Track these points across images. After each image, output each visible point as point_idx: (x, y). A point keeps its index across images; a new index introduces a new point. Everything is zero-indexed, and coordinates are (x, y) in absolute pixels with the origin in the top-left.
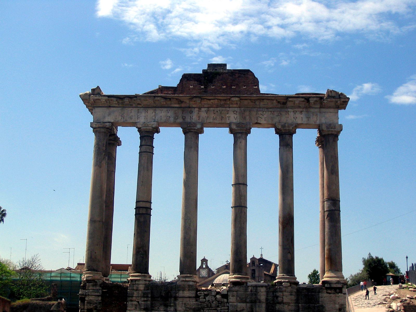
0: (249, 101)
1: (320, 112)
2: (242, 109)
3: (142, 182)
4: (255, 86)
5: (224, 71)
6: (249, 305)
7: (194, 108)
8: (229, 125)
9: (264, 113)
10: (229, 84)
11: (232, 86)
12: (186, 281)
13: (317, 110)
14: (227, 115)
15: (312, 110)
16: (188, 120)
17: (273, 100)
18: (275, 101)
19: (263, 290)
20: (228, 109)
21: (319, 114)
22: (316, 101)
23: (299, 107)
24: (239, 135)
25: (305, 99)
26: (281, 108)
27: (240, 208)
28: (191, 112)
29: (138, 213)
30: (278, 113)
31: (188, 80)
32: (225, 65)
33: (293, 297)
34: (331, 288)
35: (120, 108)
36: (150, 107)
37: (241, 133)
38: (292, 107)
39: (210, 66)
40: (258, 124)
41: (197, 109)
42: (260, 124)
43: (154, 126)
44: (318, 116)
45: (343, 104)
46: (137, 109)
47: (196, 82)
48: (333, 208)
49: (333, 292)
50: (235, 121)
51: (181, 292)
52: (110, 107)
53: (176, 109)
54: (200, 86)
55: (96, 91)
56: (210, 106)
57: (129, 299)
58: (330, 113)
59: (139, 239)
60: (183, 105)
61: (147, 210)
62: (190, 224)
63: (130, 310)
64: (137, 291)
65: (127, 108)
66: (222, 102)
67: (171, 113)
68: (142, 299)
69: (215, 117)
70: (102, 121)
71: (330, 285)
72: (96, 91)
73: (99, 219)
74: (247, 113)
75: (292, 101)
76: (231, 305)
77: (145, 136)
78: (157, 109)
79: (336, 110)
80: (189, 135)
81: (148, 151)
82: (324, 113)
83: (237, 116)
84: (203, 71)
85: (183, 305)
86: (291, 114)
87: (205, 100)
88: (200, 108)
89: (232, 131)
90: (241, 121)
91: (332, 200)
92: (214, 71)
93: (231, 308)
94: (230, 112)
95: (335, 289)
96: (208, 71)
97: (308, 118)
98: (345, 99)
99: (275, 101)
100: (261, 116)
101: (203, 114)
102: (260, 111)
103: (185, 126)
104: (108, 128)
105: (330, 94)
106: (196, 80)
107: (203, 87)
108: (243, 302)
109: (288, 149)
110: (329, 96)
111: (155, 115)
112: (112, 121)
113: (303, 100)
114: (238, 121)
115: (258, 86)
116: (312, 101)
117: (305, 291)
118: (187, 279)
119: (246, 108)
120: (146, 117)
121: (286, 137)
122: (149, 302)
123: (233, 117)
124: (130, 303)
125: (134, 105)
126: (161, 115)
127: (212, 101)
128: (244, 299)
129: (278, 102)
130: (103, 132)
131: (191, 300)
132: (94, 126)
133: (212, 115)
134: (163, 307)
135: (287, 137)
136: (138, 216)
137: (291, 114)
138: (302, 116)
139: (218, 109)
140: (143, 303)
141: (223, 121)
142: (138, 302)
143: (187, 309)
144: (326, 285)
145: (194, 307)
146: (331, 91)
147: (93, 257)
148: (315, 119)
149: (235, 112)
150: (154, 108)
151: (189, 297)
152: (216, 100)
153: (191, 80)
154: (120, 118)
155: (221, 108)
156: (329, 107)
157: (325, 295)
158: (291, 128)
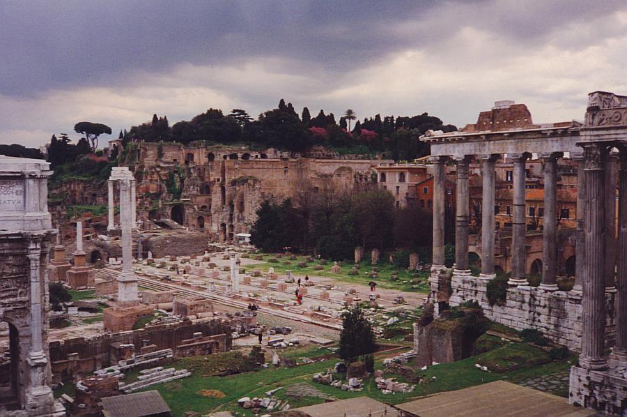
6: (519, 303)
15: (565, 138)
28: (485, 145)
41: (488, 142)
74: (520, 144)
78: (465, 144)
83: (513, 147)
86: (550, 143)
88: (489, 141)
92: (498, 108)
95: (576, 300)
97: (562, 146)
101: (492, 147)
104: (439, 161)
133: (497, 147)
137: (550, 143)
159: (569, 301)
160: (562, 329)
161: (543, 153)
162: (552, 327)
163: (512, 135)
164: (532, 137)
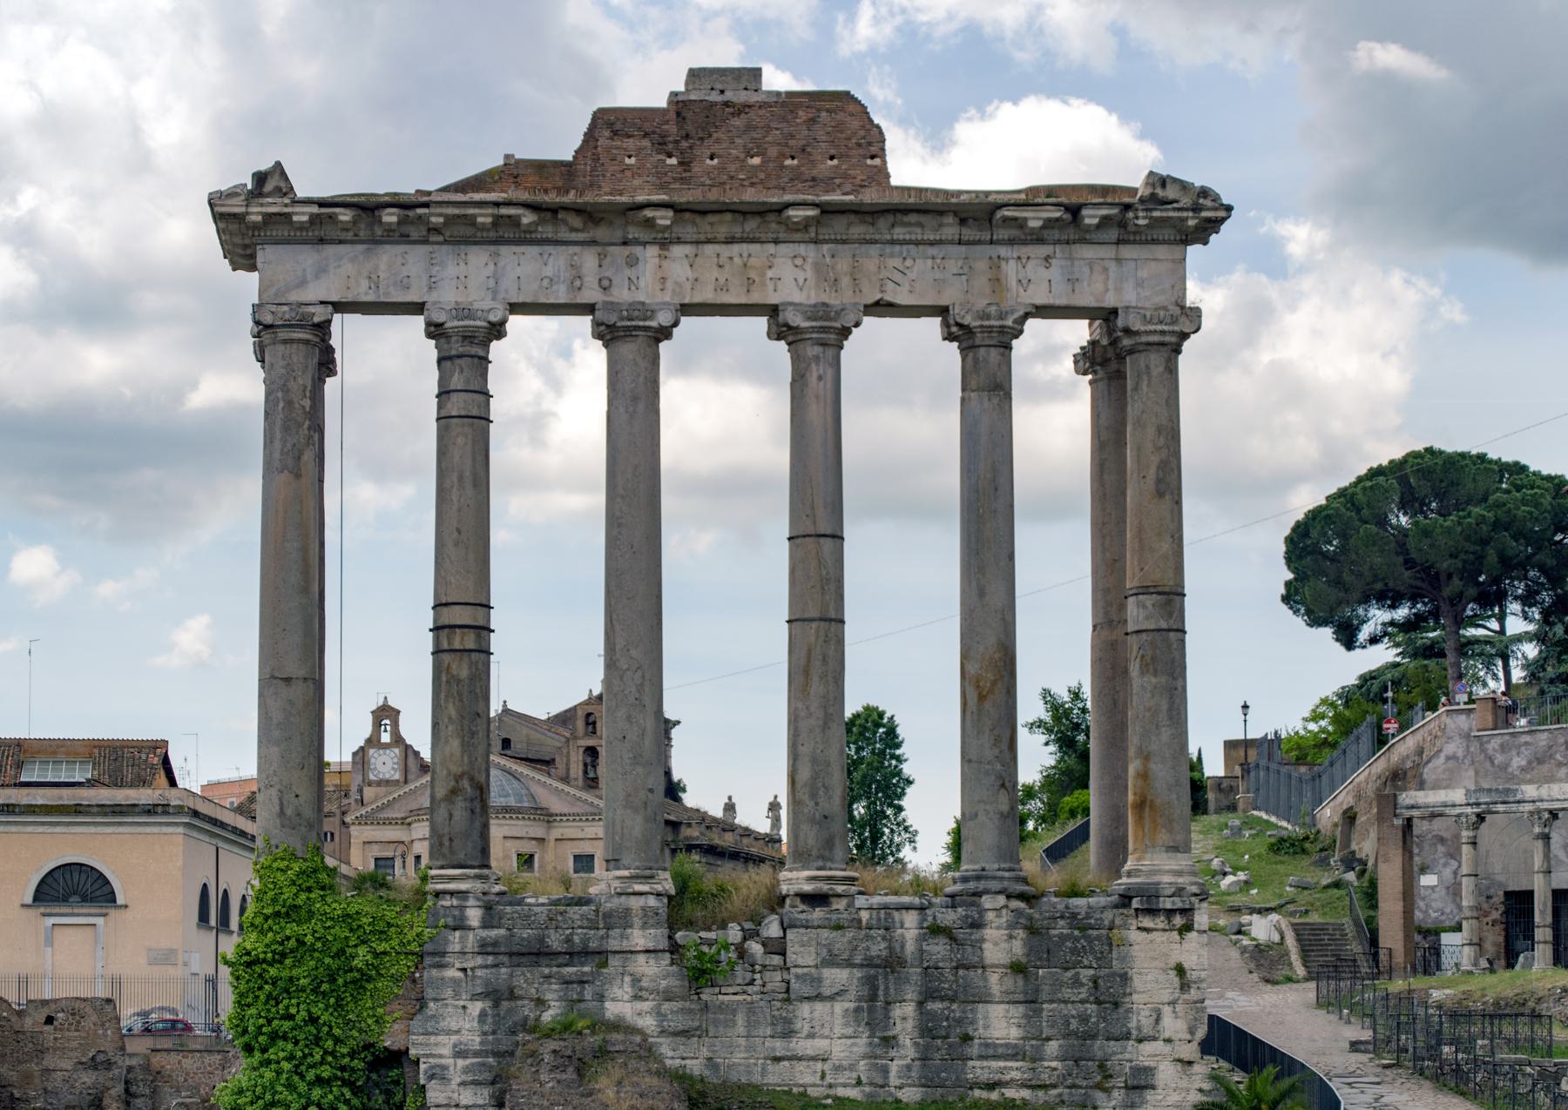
0: (852, 217)
1: (1118, 260)
2: (826, 247)
3: (459, 531)
4: (872, 157)
5: (754, 98)
6: (858, 973)
7: (644, 244)
8: (772, 311)
9: (909, 263)
10: (773, 152)
11: (783, 156)
12: (635, 894)
13: (1108, 252)
14: (770, 274)
15: (1088, 252)
16: (622, 294)
17: (941, 213)
18: (950, 219)
19: (911, 919)
20: (771, 248)
21: (1112, 266)
22: (1105, 218)
23: (1040, 241)
24: (812, 351)
25: (1067, 208)
26: (969, 243)
27: (822, 624)
28: (632, 262)
29: (445, 646)
30: (960, 263)
31: (615, 133)
32: (756, 73)
33: (1018, 948)
34: (1152, 912)
35: (360, 247)
36: (475, 243)
37: (824, 345)
38: (1011, 242)
39: (695, 75)
40: (882, 308)
41: (652, 251)
42: (890, 305)
43: (493, 318)
44: (1112, 274)
45: (1205, 229)
46: (422, 250)
47: (646, 143)
48: (1164, 625)
49: (1161, 926)
50: (798, 297)
51: (616, 932)
52: (322, 241)
53: (577, 249)
54: (662, 157)
55: (270, 181)
56: (702, 237)
57: (428, 960)
58: (1153, 264)
59: (455, 744)
60: (601, 233)
61: (478, 636)
62: (642, 685)
63: (435, 1000)
64: (457, 934)
65: (388, 247)
66: (751, 225)
67: (557, 261)
68: (479, 960)
69: (722, 281)
70: (294, 297)
71: (1148, 902)
72: (270, 181)
73: (302, 673)
75: (1016, 219)
76: (797, 976)
77: (460, 356)
78: (504, 250)
79: (1178, 248)
80: (628, 349)
81: (475, 412)
82: (1132, 264)
83: (809, 274)
84: (674, 94)
85: (627, 979)
86: (1011, 270)
87: (687, 215)
88: (664, 244)
89: (781, 331)
90: (824, 298)
91: (1159, 593)
92: (715, 97)
93: (794, 985)
94: (778, 261)
95: (1170, 913)
96: (693, 97)
97: (1072, 281)
98: (1216, 209)
99: (950, 219)
100: (897, 277)
102: (892, 256)
103: (612, 319)
105: (1159, 191)
106: (646, 135)
107: (674, 161)
108: (838, 965)
109: (995, 401)
110: (1153, 201)
111: (495, 272)
112: (335, 299)
113: (1058, 215)
114: (809, 296)
115: (884, 162)
116: (1090, 217)
117: (1061, 923)
118: (638, 888)
119: (840, 247)
120: (462, 282)
121: (984, 348)
122: (503, 970)
123: (791, 276)
124: (434, 972)
125: (415, 234)
126: (519, 271)
127: (711, 218)
128: (845, 956)
129: (963, 222)
130: (300, 341)
131: (652, 962)
132: (268, 319)
134: (555, 987)
135: (994, 353)
136: (446, 658)
138: (1046, 274)
139: (736, 248)
140: (479, 973)
141: (756, 298)
142: (464, 970)
143: (644, 994)
144: (1135, 903)
145: (664, 983)
146: (1164, 181)
147: (289, 812)
148: (1099, 287)
149: (799, 262)
150: (492, 248)
151: (647, 951)
152: (728, 216)
153: (629, 137)
154: (364, 284)
155: (745, 246)
156: (1154, 241)
157: (1134, 935)
158: (1009, 322)
159: (1134, 923)
160: (1098, 1047)
161: (981, 304)
162: (1053, 1047)
163: (827, 210)
164: (918, 234)
